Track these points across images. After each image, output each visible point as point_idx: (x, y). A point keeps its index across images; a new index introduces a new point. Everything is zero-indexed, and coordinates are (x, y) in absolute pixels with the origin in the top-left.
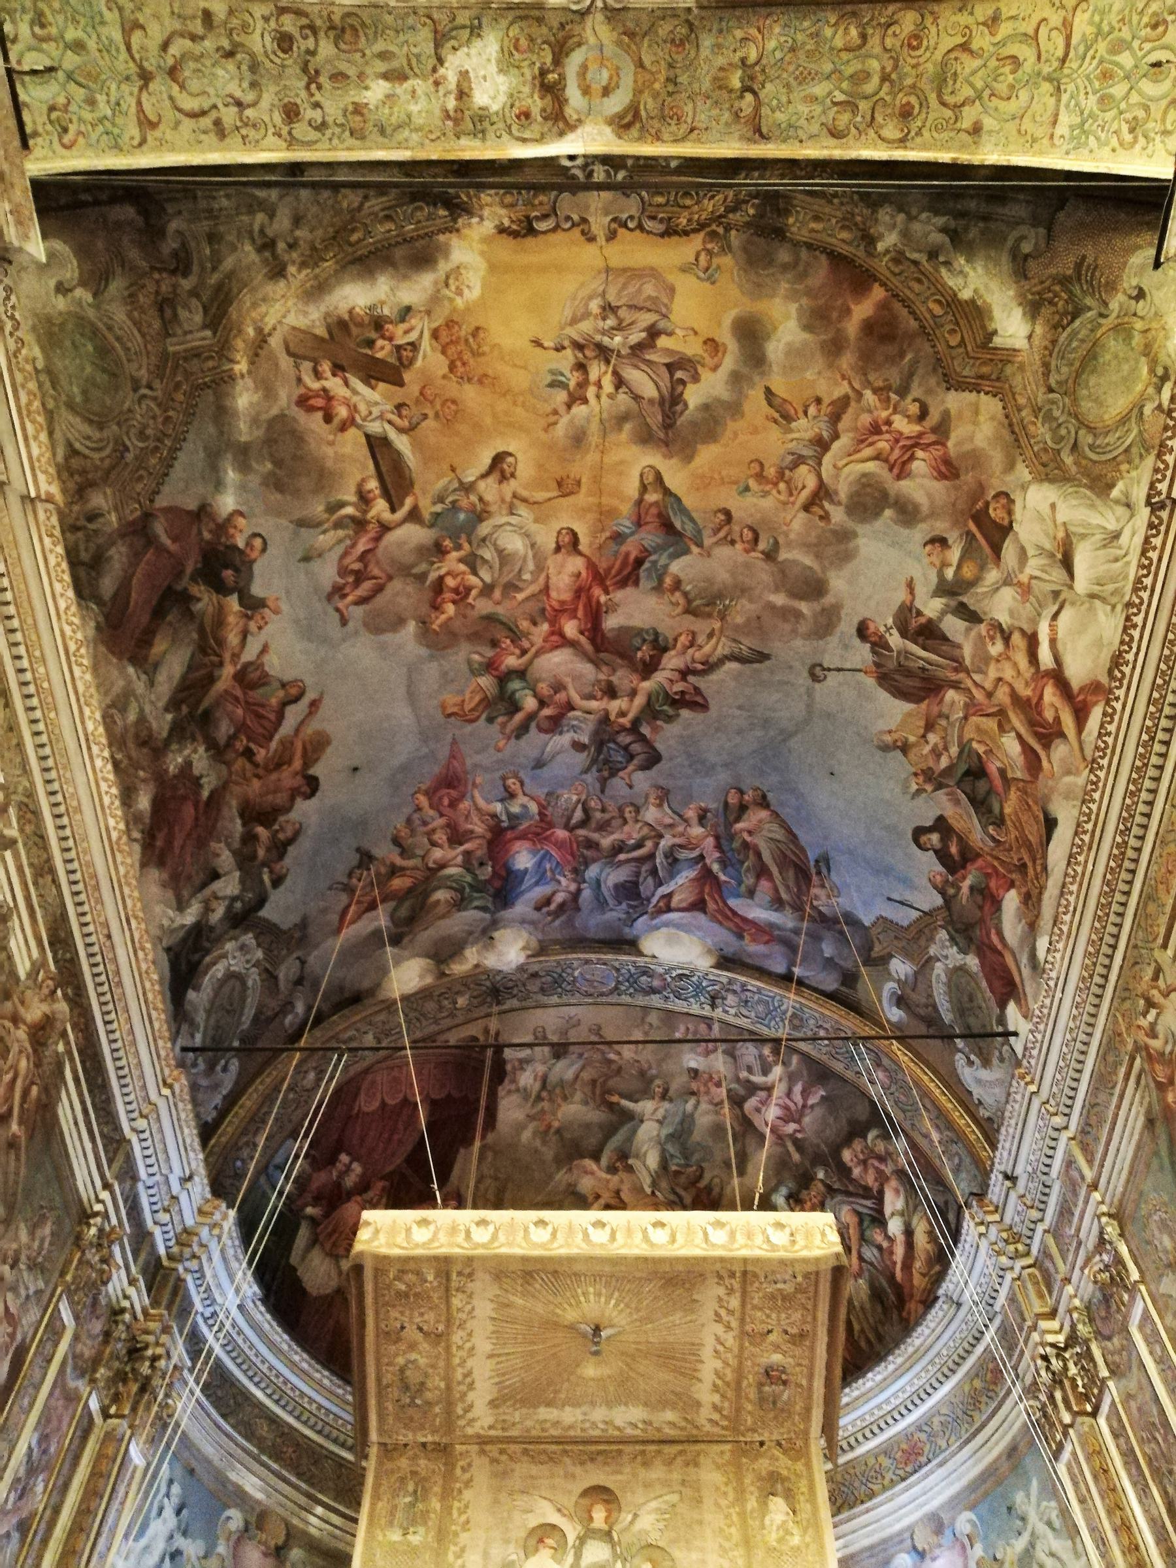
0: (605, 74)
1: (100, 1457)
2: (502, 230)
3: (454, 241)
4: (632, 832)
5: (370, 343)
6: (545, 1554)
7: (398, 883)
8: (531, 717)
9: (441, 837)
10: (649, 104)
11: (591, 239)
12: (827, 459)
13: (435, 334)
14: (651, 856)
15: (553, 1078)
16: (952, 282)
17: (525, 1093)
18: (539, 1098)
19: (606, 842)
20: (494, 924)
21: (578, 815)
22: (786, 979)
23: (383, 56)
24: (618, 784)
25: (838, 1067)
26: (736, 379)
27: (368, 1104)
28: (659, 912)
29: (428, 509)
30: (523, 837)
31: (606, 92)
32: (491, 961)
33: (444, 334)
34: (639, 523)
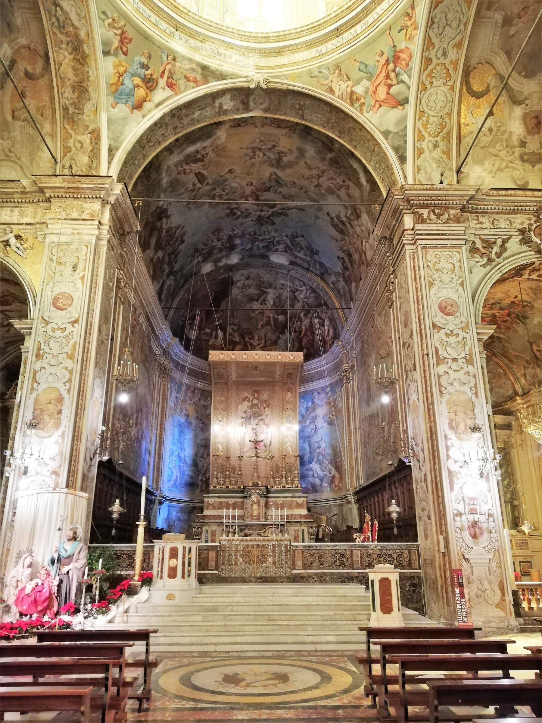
0: (261, 101)
1: (163, 389)
2: (231, 126)
3: (217, 130)
4: (268, 237)
5: (196, 156)
6: (246, 402)
7: (204, 252)
8: (239, 216)
9: (215, 240)
10: (273, 107)
11: (257, 127)
12: (320, 179)
13: (213, 150)
14: (273, 241)
15: (246, 284)
16: (352, 163)
17: (239, 288)
18: (242, 288)
19: (260, 238)
20: (230, 254)
21: (253, 233)
22: (308, 269)
23: (199, 106)
24: (264, 228)
25: (318, 291)
26: (297, 158)
27: (199, 296)
28: (274, 251)
29: (210, 181)
30: (238, 237)
31: (261, 104)
32: (229, 262)
33: (215, 150)
34: (270, 181)
